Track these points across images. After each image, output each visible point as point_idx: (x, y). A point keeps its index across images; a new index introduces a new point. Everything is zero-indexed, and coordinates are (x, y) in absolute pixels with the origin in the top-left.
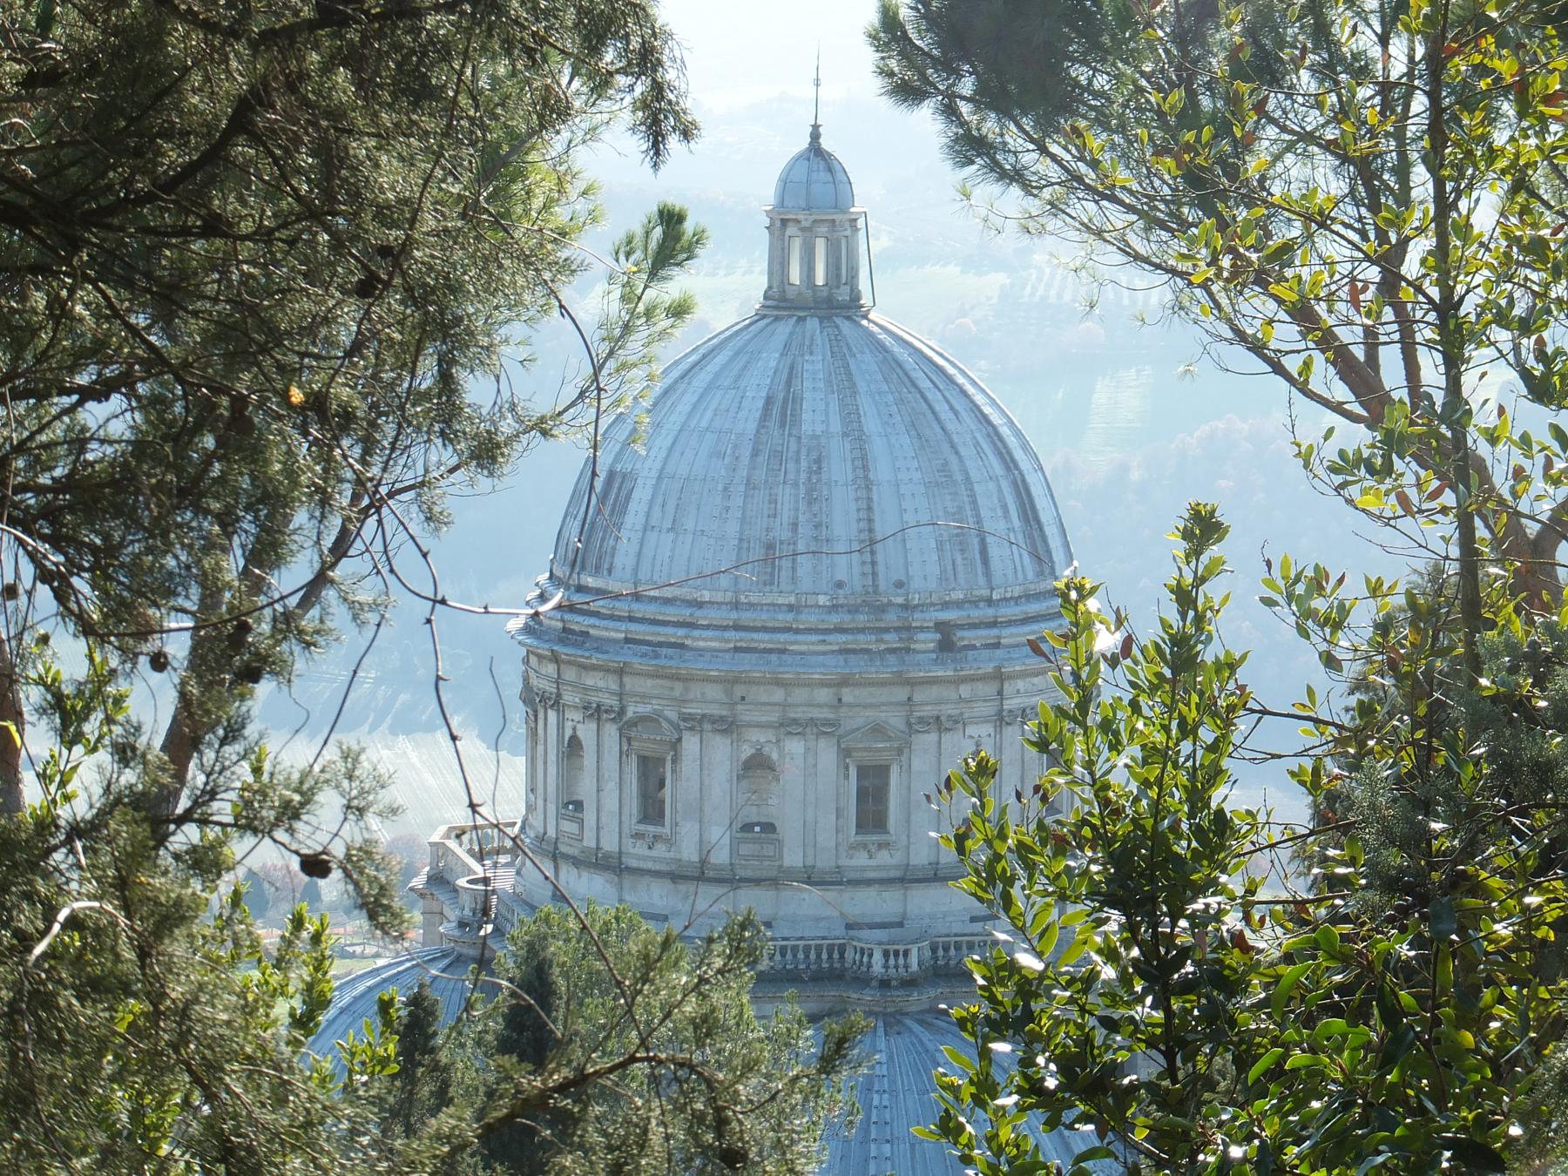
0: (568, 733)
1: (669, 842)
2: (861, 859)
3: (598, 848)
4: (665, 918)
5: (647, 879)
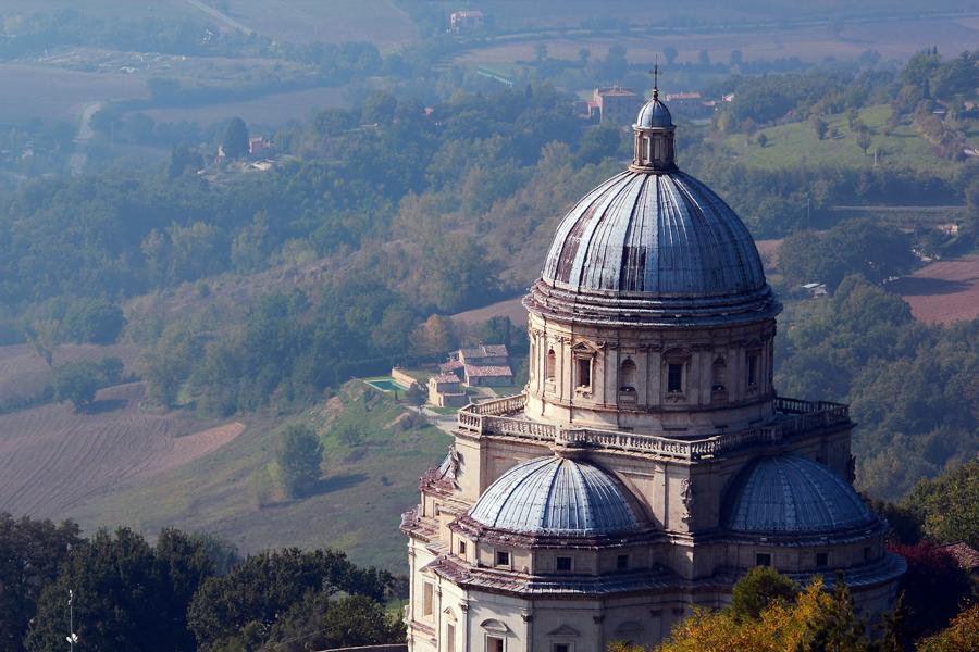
0: (624, 358)
1: (684, 398)
2: (750, 396)
3: (648, 405)
4: (686, 429)
5: (673, 415)
